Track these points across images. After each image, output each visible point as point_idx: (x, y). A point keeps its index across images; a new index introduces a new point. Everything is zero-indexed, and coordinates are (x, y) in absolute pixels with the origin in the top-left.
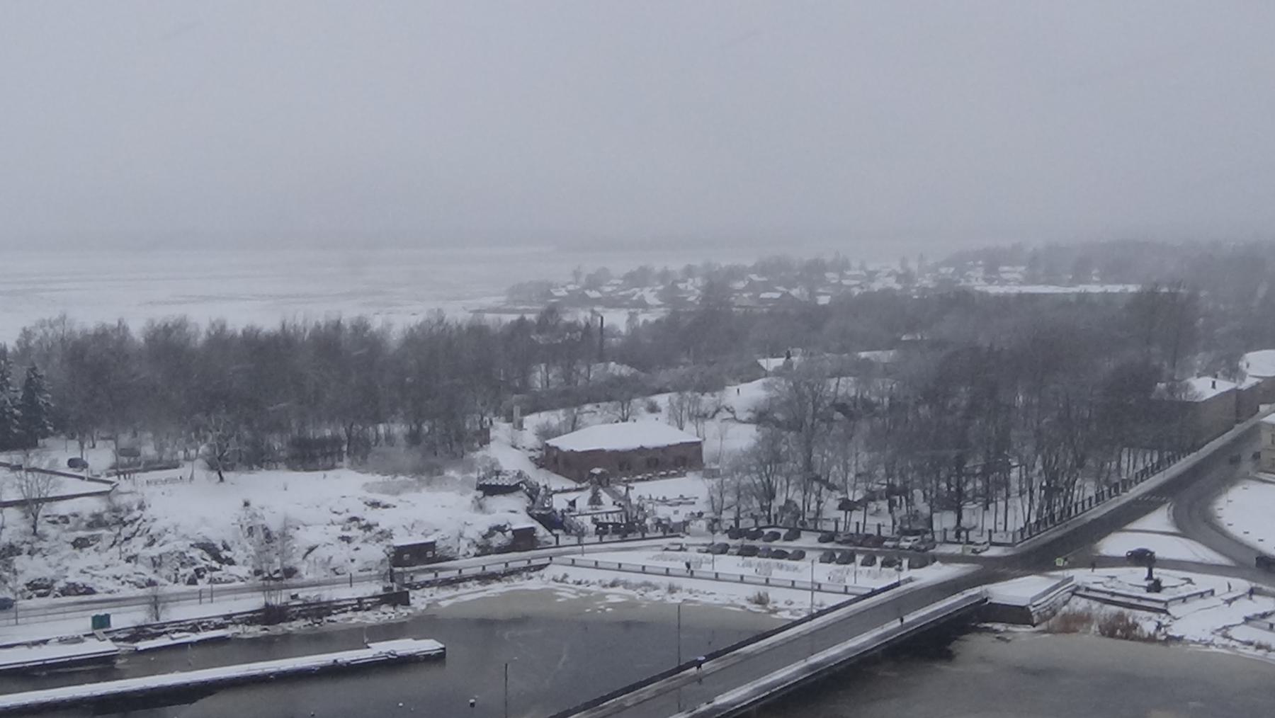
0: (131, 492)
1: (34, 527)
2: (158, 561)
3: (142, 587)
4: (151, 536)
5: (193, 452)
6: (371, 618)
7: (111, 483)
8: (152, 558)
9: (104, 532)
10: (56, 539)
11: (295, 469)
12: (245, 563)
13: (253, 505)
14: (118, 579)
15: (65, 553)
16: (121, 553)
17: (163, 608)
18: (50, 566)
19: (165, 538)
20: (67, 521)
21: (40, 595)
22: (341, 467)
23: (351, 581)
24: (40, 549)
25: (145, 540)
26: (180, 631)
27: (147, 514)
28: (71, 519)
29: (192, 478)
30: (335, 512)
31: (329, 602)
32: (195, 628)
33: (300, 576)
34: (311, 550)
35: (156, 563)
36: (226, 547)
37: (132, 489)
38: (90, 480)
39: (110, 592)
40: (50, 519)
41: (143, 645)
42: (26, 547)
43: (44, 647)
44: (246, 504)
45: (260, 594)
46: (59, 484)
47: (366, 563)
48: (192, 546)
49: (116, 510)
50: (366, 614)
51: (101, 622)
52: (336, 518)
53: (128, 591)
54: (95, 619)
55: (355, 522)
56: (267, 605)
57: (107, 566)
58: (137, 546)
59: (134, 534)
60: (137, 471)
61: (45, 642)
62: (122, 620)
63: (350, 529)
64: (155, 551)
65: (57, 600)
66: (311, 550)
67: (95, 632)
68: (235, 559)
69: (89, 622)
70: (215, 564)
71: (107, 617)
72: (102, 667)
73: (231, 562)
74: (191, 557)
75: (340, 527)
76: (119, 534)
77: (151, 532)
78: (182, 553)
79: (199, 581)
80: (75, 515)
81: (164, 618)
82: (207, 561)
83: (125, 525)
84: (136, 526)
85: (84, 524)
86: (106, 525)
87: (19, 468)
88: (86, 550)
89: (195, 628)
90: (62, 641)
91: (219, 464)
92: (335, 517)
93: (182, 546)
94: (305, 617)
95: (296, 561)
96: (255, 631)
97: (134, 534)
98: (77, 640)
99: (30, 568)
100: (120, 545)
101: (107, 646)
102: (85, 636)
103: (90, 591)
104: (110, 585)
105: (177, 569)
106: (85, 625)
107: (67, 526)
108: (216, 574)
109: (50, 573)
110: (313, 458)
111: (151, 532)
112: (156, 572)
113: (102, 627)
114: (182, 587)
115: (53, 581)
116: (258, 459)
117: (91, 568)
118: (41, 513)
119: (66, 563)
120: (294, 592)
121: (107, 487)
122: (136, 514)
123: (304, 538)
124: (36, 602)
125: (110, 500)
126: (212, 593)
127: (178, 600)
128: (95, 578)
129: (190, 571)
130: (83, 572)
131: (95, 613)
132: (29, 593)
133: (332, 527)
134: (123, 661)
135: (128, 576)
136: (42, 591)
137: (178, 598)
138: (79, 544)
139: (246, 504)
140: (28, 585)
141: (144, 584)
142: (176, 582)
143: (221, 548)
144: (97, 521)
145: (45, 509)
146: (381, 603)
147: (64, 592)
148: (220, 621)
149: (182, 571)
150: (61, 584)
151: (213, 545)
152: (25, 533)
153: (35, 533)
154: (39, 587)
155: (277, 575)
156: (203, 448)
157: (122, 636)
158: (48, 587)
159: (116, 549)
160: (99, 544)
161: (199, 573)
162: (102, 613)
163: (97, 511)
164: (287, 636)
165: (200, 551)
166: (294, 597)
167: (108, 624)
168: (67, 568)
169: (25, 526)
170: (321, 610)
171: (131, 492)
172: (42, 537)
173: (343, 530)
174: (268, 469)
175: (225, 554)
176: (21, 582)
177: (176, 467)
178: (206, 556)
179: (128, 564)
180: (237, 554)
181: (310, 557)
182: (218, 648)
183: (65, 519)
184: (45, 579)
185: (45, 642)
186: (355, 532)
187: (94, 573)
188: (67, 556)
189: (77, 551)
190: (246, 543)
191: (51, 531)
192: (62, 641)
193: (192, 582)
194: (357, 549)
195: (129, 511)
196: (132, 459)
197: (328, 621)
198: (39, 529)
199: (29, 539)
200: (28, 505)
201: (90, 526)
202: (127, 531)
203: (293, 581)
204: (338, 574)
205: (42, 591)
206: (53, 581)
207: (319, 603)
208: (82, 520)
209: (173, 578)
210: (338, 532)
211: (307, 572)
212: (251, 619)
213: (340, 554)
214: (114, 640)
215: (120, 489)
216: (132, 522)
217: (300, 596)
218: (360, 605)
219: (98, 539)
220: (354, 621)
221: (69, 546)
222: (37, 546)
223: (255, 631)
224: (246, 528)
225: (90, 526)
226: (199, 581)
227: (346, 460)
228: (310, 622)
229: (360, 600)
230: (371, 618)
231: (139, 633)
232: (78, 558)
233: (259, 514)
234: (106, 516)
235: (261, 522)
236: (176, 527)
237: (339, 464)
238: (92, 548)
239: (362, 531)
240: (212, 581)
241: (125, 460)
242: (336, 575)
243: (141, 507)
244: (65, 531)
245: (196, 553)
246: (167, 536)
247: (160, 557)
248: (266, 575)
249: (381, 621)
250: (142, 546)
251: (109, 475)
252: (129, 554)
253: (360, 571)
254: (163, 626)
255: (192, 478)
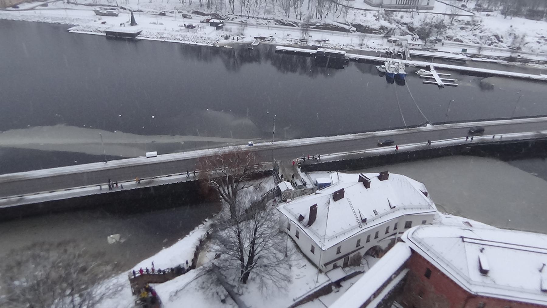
0: (479, 17)
1: (452, 21)
2: (482, 37)
3: (475, 43)
4: (482, 30)
5: (497, 9)
6: (541, 67)
7: (474, 13)
8: (480, 36)
9: (469, 26)
10: (456, 26)
11: (527, 18)
12: (506, 43)
13: (513, 27)
14: (470, 40)
15: (457, 30)
16: (472, 33)
17: (482, 50)
18: (453, 33)
19: (485, 32)
20: (460, 22)
21: (448, 40)
22: (542, 20)
23: (537, 55)
24: (451, 28)
25: (480, 31)
26: (485, 58)
27: (482, 24)
28: (461, 21)
29: (497, 16)
30: (538, 34)
31: (530, 60)
32: (489, 58)
33: (521, 50)
34: (527, 43)
35: (481, 38)
36: (502, 38)
37: (480, 16)
38: (468, 11)
39: (467, 43)
40: (456, 20)
41: (474, 59)
42: (448, 27)
43: (449, 54)
44: (511, 26)
45: (510, 53)
46: (462, 11)
47: (542, 51)
48: (492, 35)
49: (474, 21)
50: (540, 65)
51: (464, 51)
52: (537, 35)
53: (471, 44)
54: (463, 49)
55: (543, 38)
56: (511, 56)
57: (468, 36)
58: (477, 32)
59: (477, 29)
60: (480, 11)
61: (449, 52)
62: (470, 51)
63: (541, 40)
64: (482, 34)
65: (453, 42)
66: (527, 43)
67: (462, 53)
68: (504, 41)
69: (461, 50)
70: (497, 41)
71: (466, 49)
72: (462, 62)
73: (502, 42)
74: (491, 38)
75: (537, 39)
76: (473, 28)
77: (482, 29)
78: (489, 37)
79: (491, 45)
80: (462, 20)
81: (481, 53)
82: (494, 39)
83: (475, 26)
84: (478, 26)
85: (464, 23)
86: (470, 25)
87: (448, 5)
88: (463, 30)
89: (489, 58)
90: (453, 53)
91: (505, 13)
92: (537, 35)
93: (490, 35)
94: (521, 62)
95: (521, 46)
96: (505, 62)
97: (477, 29)
98: (457, 54)
99: (450, 33)
100: (473, 31)
101: (465, 57)
102: (460, 53)
103: (462, 42)
104: (467, 41)
105: (486, 41)
106: (459, 50)
107: (460, 23)
108: (496, 44)
109: (453, 35)
110: (533, 16)
111: (482, 29)
112: (480, 40)
113: (464, 52)
114: (486, 46)
115: (453, 37)
116: (516, 13)
117: (463, 35)
118: (455, 18)
119: (457, 33)
120: (519, 54)
121: (472, 14)
122: (479, 23)
123: (527, 39)
124: (447, 41)
125: (473, 18)
126: (495, 49)
127: (485, 49)
128: (464, 39)
129: (490, 42)
130: (461, 36)
131: (463, 48)
132: (446, 39)
133: (535, 38)
134: (468, 62)
135: (473, 40)
136: (450, 39)
137: (485, 49)
138: (462, 28)
139: (511, 26)
140: (446, 37)
141: (476, 43)
142: (485, 44)
143: (500, 37)
144: (468, 23)
145: (456, 18)
146: (545, 63)
147: (455, 40)
148: (496, 57)
149: (487, 41)
150: (455, 38)
151: (498, 36)
152: (449, 23)
153: (451, 23)
154: (449, 38)
155: (515, 48)
156: (501, 8)
157: (469, 55)
158: (451, 38)
159: (471, 32)
160: (467, 30)
161: (492, 43)
162: (465, 48)
163: (469, 20)
164: (514, 66)
165: (494, 37)
166: (519, 56)
167: (466, 52)
168: (457, 34)
169: (449, 21)
170: (526, 61)
171: (479, 17)
172: (453, 25)
173: (539, 39)
174: (519, 17)
175: (501, 39)
176: (445, 36)
177: (492, 12)
178: (496, 39)
179: (474, 37)
180: (504, 40)
181: (526, 45)
182: (494, 65)
183: (460, 21)
184: (451, 36)
185: (449, 52)
186: (542, 41)
187: (464, 37)
188: (457, 31)
189: (461, 30)
190: (508, 37)
191: (456, 24)
192: (453, 53)
193: (490, 45)
194: (541, 46)
195: (477, 22)
196: (480, 8)
197: (528, 65)
198: (453, 22)
199: (450, 24)
200: (452, 15)
201: (466, 24)
202: (476, 27)
203: (519, 51)
204: (533, 52)
205: (450, 39)
206: (453, 37)
207: (526, 59)
208: (464, 22)
209: (485, 43)
210: (537, 39)
211: (524, 50)
212: (506, 59)
213: (535, 46)
214: (467, 56)
215: (475, 15)
216: (477, 25)
217: (521, 56)
218: (538, 62)
219: (467, 28)
220: (535, 66)
221: (459, 28)
222: (451, 27)
223: (505, 62)
224: (509, 33)
225: (466, 24)
226: (491, 45)
227: (544, 18)
228: (521, 64)
229: (539, 61)
230: (541, 67)
231: (473, 56)
232: (460, 32)
233: (514, 30)
234: (471, 22)
235: (514, 32)
236: (489, 29)
237: (542, 19)
238: (464, 30)
239: (544, 41)
240: (495, 46)
241: (478, 7)
242: (533, 52)
243: (481, 22)
244: (459, 24)
245: (493, 37)
246: (486, 31)
247: (483, 36)
248: (511, 48)
249: (544, 69)
250: (478, 32)
251: (473, 11)
252: (474, 34)
253: (541, 52)
254: (481, 55)
255: (497, 16)
